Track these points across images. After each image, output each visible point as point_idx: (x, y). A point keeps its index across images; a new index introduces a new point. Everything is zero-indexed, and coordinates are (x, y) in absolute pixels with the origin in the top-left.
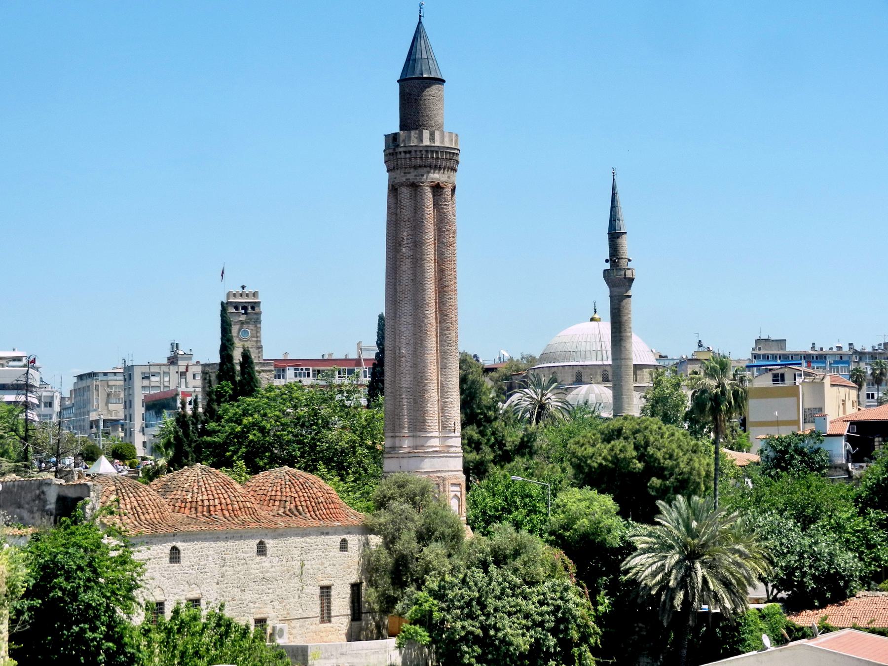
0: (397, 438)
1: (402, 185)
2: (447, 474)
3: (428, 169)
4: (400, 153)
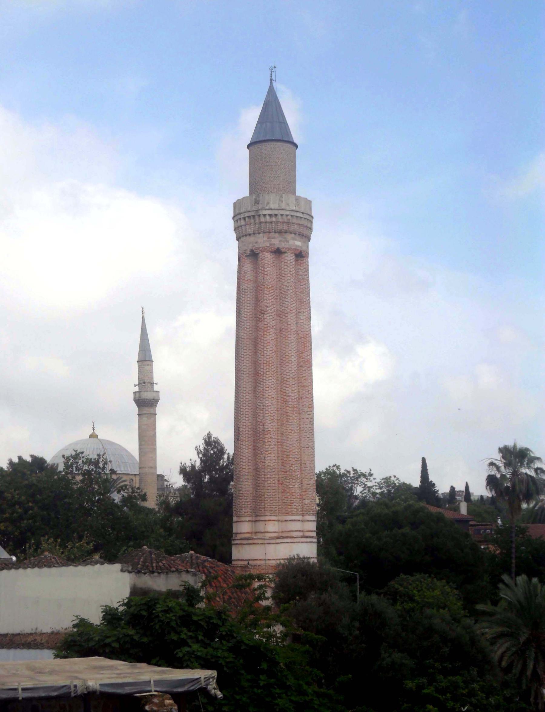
0: (258, 524)
1: (264, 250)
2: (259, 562)
3: (293, 235)
4: (265, 215)
